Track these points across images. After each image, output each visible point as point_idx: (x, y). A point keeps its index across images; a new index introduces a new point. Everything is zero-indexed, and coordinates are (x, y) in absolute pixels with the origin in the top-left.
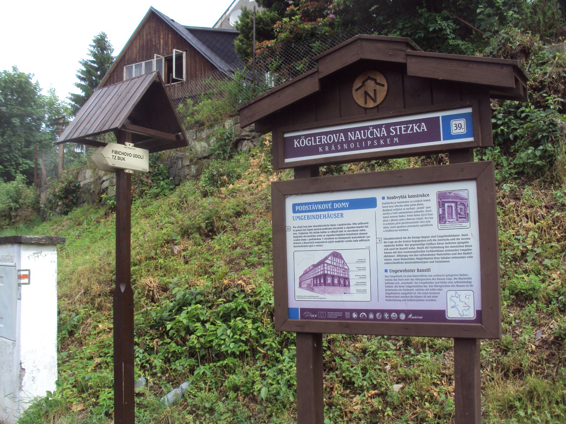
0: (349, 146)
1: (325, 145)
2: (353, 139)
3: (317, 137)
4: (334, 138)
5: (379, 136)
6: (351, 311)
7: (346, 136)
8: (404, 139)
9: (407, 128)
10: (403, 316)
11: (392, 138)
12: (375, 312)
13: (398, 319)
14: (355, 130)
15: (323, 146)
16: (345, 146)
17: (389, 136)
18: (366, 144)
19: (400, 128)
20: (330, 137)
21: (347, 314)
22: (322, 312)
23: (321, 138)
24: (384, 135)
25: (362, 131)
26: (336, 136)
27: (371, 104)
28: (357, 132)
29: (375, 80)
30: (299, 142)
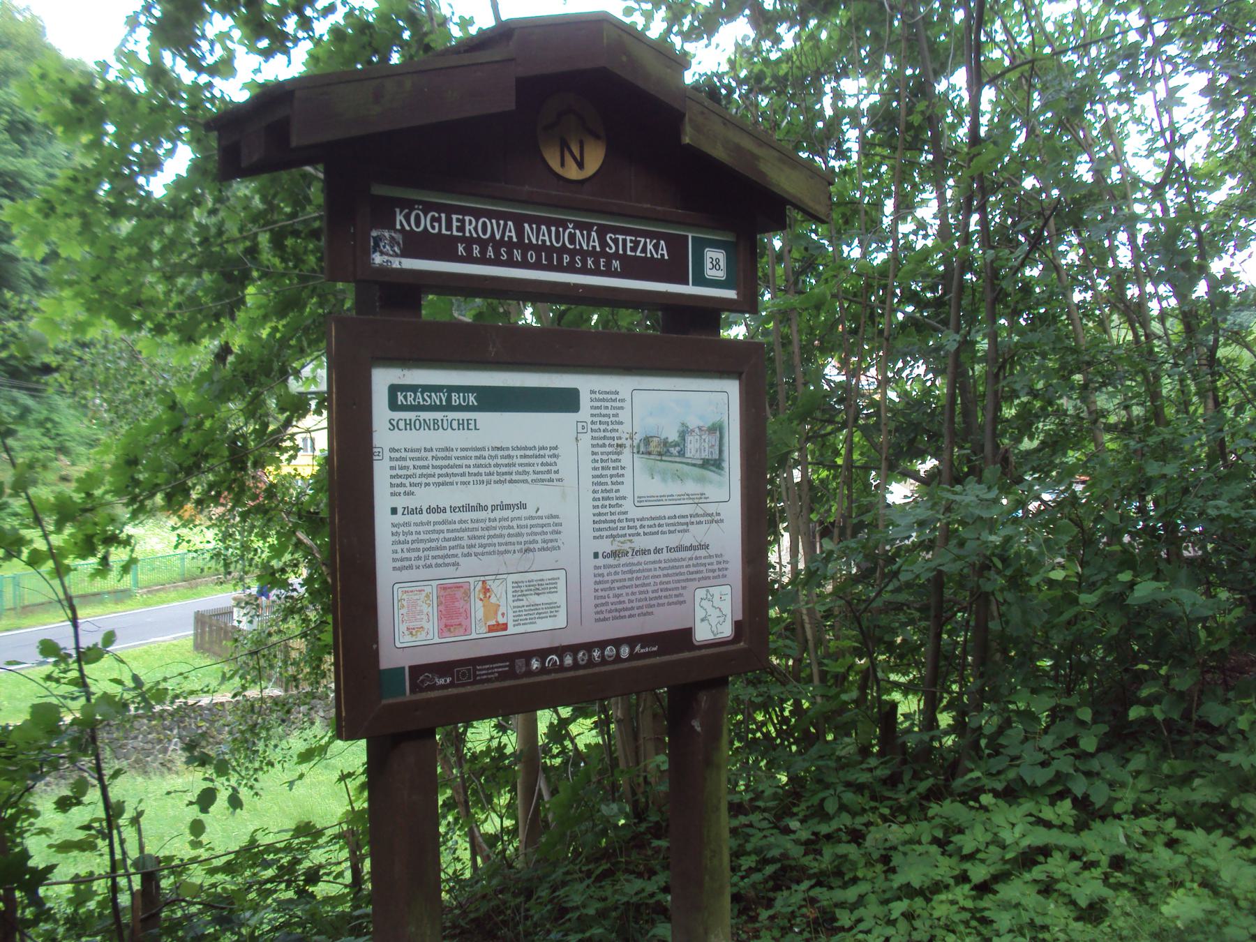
0: (524, 256)
2: (534, 241)
3: (454, 217)
5: (585, 247)
6: (528, 655)
7: (520, 232)
9: (636, 243)
10: (625, 651)
11: (610, 258)
12: (574, 649)
13: (618, 658)
15: (469, 242)
16: (517, 255)
17: (603, 253)
18: (560, 259)
19: (624, 241)
20: (484, 224)
21: (520, 662)
22: (463, 669)
23: (463, 221)
24: (594, 247)
25: (553, 229)
26: (498, 225)
28: (543, 227)
30: (407, 218)
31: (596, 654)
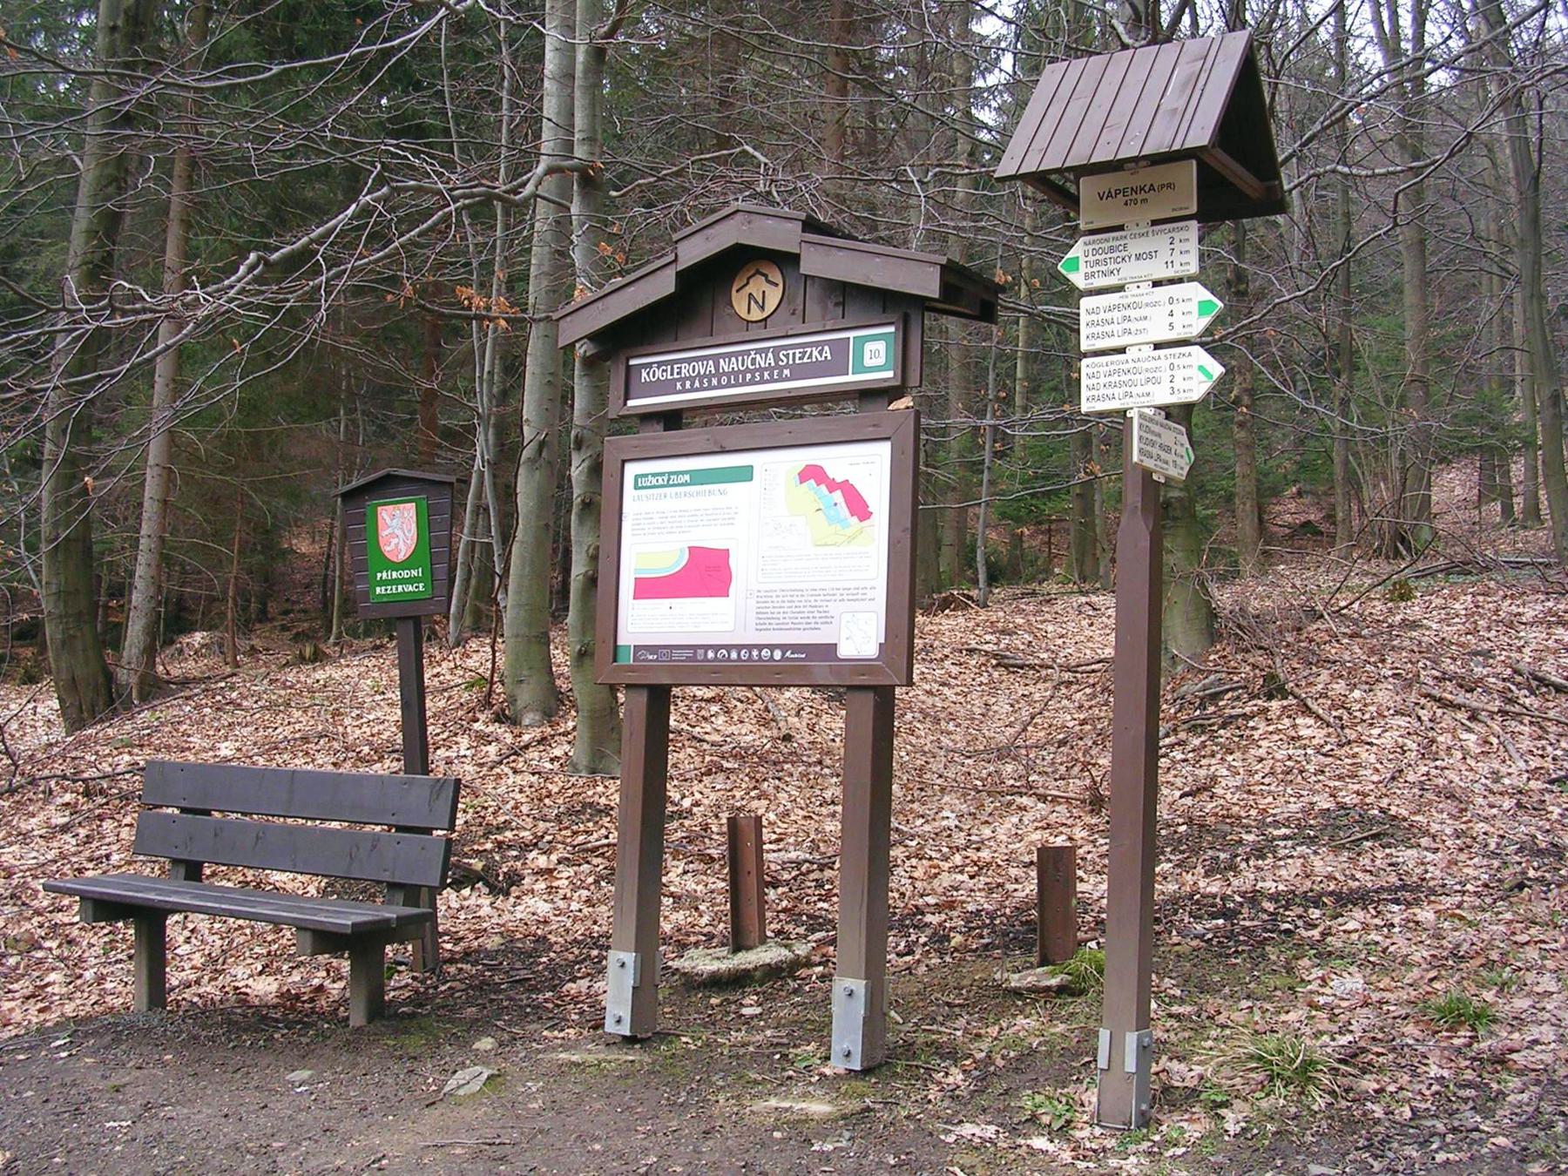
1: (687, 378)
4: (700, 368)
7: (717, 366)
8: (799, 372)
14: (729, 355)
18: (744, 378)
27: (756, 315)
29: (766, 276)
31: (755, 653)
